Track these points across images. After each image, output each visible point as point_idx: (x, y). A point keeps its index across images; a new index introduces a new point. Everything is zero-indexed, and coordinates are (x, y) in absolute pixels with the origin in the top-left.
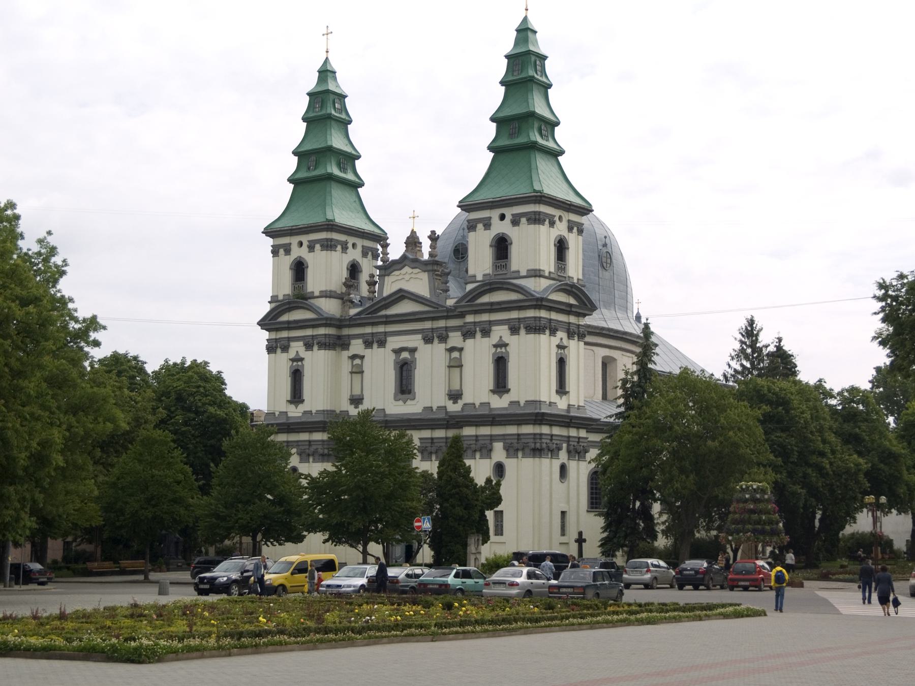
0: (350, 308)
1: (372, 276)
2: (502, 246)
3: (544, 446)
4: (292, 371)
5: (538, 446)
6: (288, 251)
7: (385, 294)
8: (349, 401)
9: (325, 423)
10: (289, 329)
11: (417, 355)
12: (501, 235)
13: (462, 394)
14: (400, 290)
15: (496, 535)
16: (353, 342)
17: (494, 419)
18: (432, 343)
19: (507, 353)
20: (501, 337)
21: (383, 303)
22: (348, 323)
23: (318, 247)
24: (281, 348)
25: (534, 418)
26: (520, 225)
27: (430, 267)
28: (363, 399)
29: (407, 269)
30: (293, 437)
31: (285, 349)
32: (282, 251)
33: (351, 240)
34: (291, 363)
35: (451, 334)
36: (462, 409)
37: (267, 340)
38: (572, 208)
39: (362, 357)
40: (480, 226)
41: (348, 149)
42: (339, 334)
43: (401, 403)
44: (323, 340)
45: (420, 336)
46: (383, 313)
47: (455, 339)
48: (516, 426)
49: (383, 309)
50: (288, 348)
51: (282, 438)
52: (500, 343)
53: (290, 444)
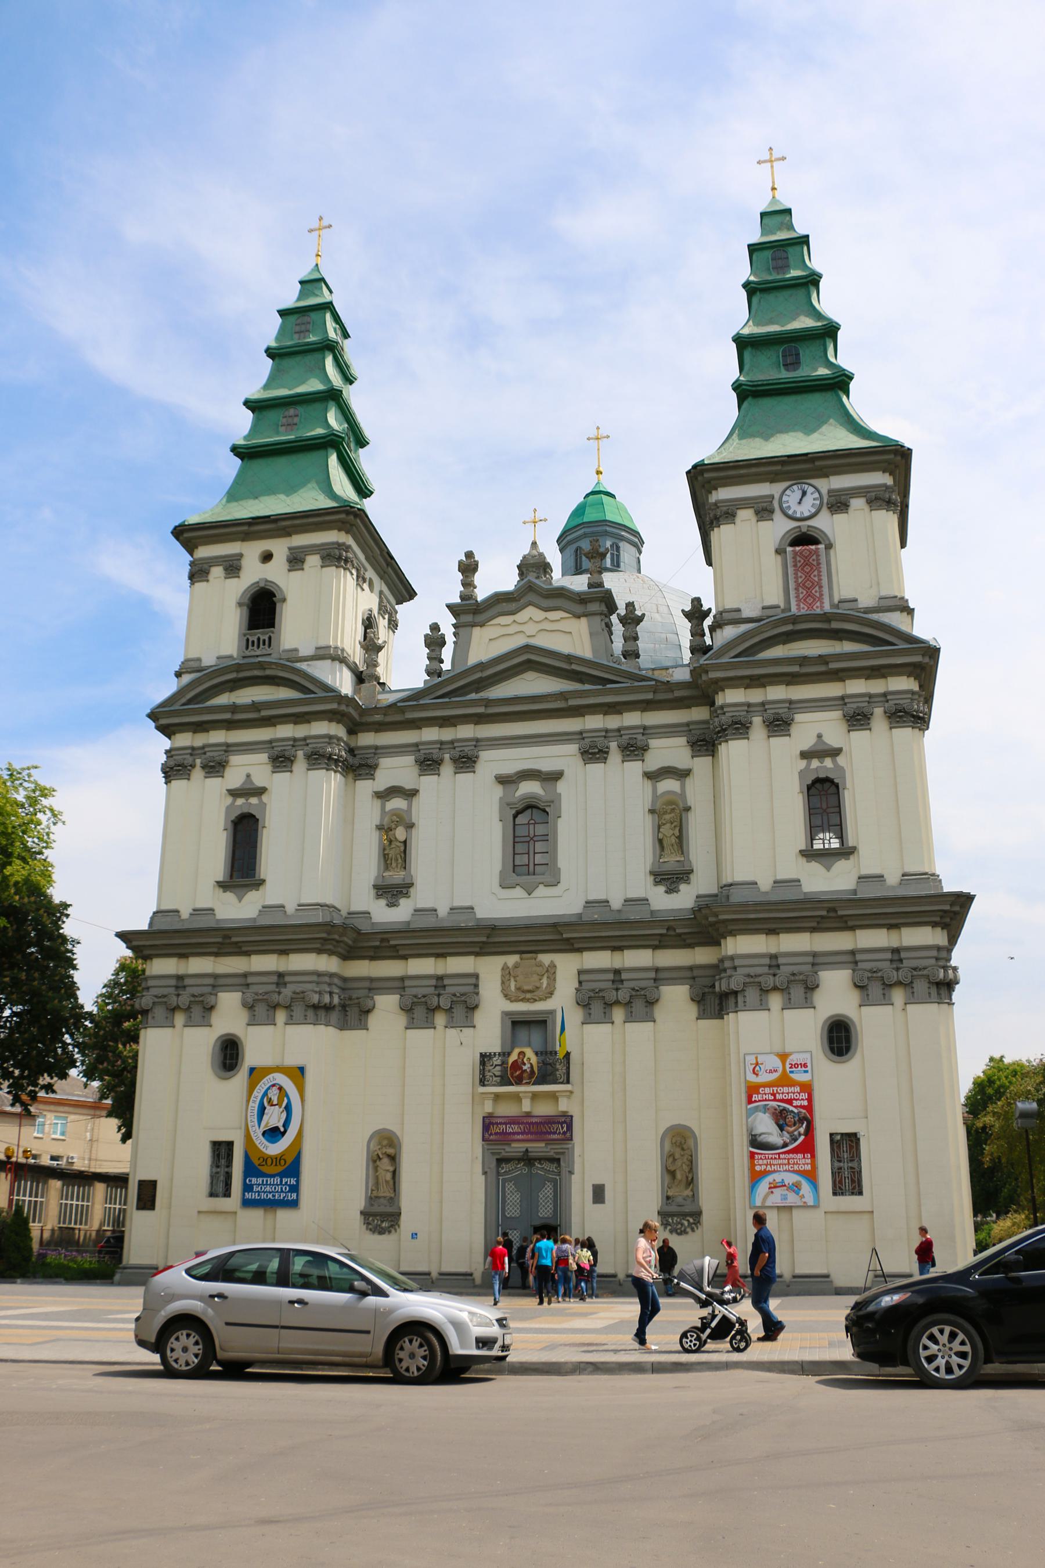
1: (435, 627)
4: (233, 818)
6: (232, 567)
8: (373, 892)
10: (230, 725)
11: (561, 786)
12: (804, 530)
14: (527, 648)
15: (835, 1194)
16: (385, 762)
18: (606, 759)
20: (820, 736)
22: (378, 718)
23: (313, 561)
24: (203, 767)
26: (851, 510)
27: (594, 607)
28: (411, 885)
32: (217, 572)
34: (230, 800)
35: (653, 743)
37: (167, 752)
39: (411, 794)
40: (745, 515)
42: (353, 745)
43: (519, 892)
45: (573, 748)
46: (473, 696)
49: (472, 693)
50: (224, 767)
51: (199, 965)
52: (820, 747)
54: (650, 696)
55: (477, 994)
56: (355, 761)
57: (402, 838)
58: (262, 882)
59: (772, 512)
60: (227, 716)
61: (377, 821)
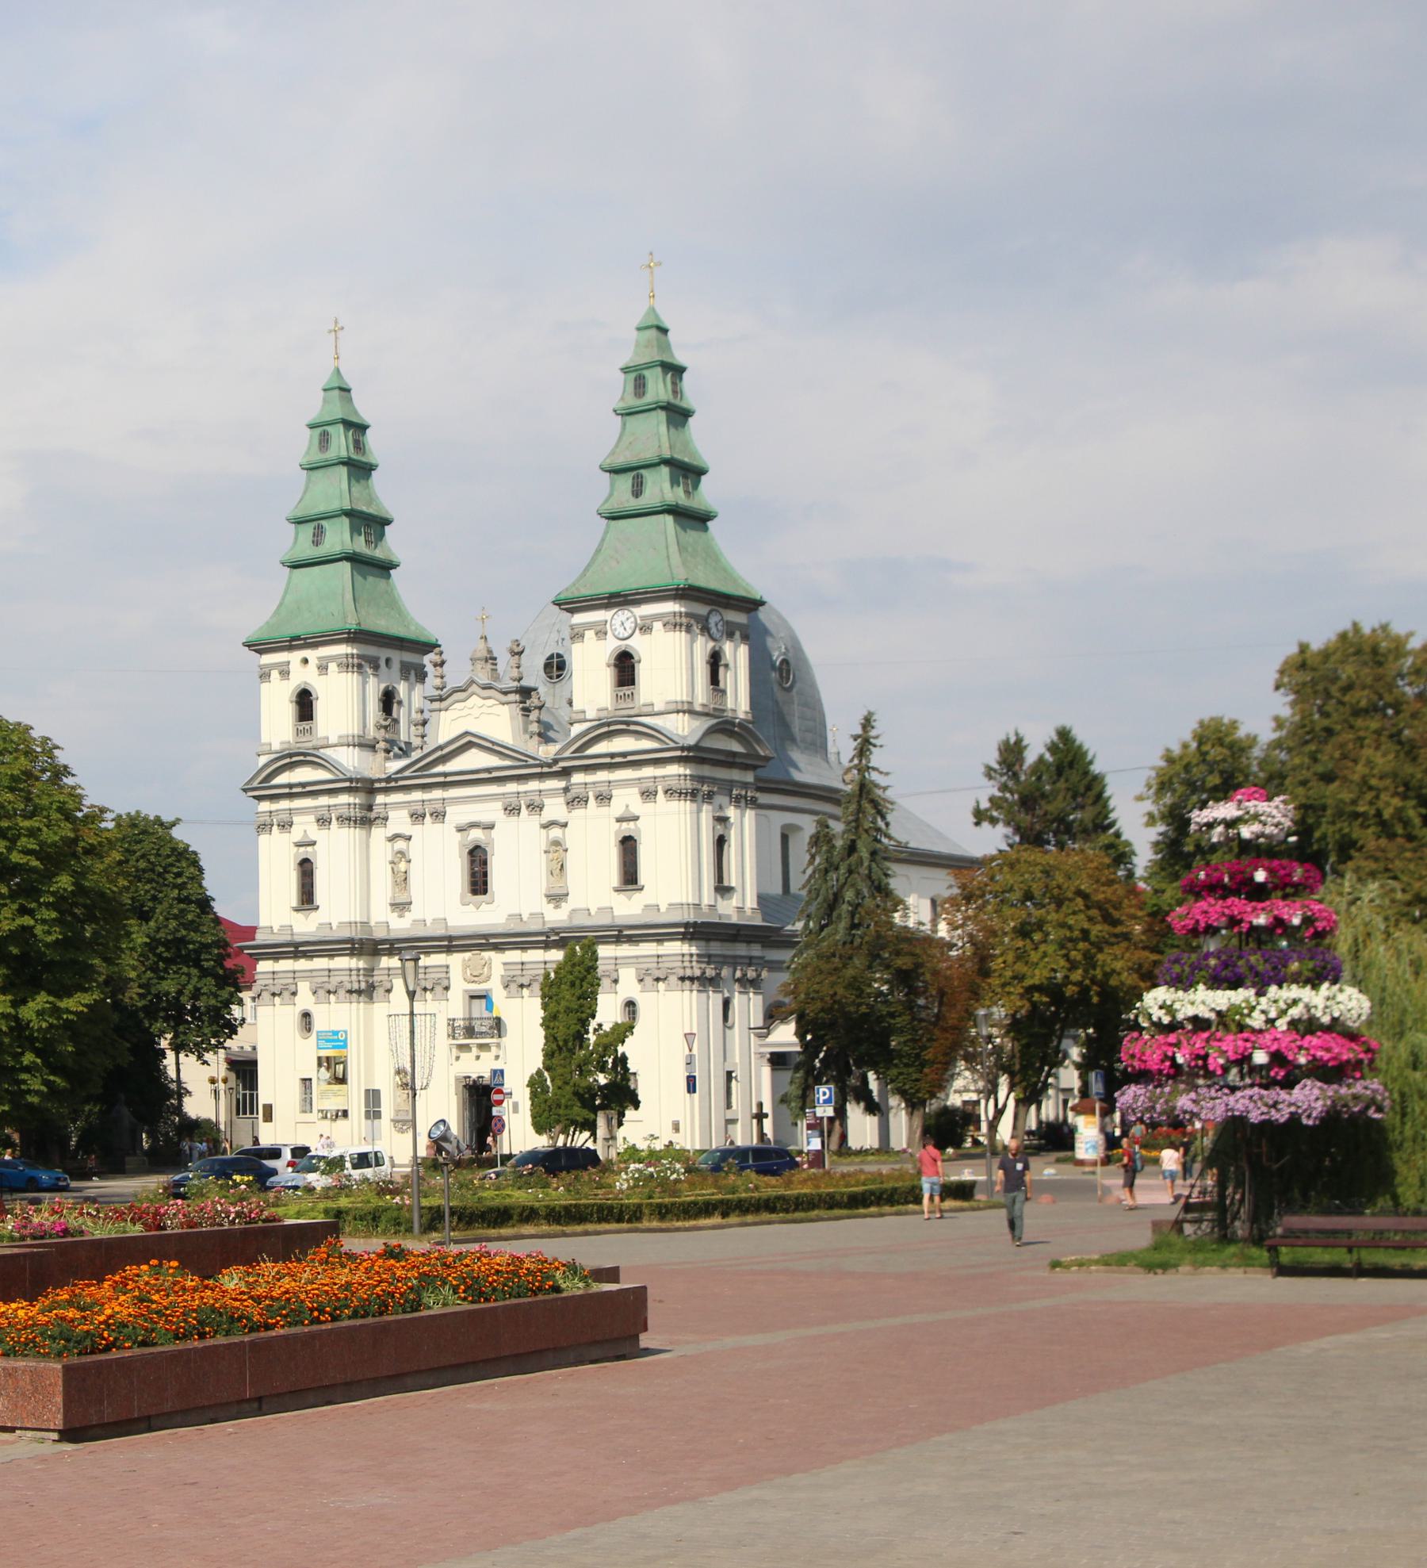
0: (387, 759)
2: (625, 667)
3: (698, 973)
5: (689, 973)
7: (441, 741)
9: (351, 941)
10: (291, 796)
13: (567, 895)
14: (467, 733)
17: (621, 935)
19: (638, 830)
20: (627, 806)
21: (439, 753)
22: (383, 785)
23: (333, 667)
25: (682, 930)
28: (411, 903)
29: (475, 700)
30: (302, 964)
31: (286, 826)
32: (275, 674)
33: (383, 654)
35: (547, 801)
36: (570, 917)
38: (732, 602)
39: (409, 838)
40: (590, 634)
41: (371, 510)
44: (345, 812)
45: (499, 805)
46: (440, 769)
47: (555, 808)
48: (655, 944)
53: (297, 975)
54: (538, 770)
55: (449, 978)
56: (373, 815)
57: (403, 870)
58: (317, 908)
59: (606, 634)
60: (287, 790)
61: (390, 858)
